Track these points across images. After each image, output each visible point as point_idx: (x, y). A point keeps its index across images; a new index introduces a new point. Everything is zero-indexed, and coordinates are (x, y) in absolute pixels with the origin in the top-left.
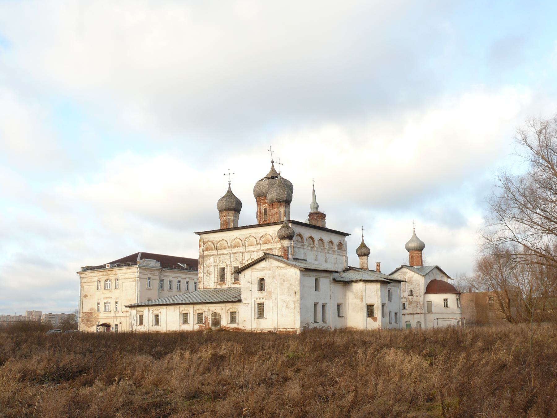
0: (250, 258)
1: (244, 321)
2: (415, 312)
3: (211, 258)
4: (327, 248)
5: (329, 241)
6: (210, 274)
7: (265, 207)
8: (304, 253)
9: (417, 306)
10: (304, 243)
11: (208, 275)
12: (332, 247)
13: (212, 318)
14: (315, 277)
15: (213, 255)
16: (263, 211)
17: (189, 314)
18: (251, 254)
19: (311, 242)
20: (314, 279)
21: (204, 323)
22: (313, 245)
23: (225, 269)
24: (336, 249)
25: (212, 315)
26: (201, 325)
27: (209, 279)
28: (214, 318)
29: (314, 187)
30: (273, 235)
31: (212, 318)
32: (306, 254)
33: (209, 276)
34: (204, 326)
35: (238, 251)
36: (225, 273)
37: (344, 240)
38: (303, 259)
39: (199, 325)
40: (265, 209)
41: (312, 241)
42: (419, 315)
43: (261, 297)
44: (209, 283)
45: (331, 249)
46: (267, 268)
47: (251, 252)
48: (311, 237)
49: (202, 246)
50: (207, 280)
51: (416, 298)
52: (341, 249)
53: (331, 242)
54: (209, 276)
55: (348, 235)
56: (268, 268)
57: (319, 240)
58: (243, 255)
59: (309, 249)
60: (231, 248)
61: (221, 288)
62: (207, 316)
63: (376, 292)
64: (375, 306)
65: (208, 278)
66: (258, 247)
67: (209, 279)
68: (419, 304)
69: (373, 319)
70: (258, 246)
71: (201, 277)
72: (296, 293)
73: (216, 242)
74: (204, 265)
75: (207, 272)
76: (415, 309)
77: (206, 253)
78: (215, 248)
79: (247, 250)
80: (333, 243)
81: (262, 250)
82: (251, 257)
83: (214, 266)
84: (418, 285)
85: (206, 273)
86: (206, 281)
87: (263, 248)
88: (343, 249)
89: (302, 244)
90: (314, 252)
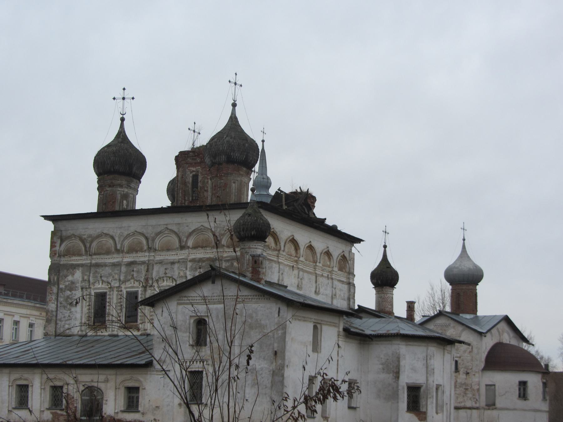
0: (164, 275)
1: (157, 407)
2: (462, 405)
3: (78, 271)
4: (321, 265)
5: (324, 251)
7: (194, 173)
8: (279, 272)
9: (466, 394)
10: (281, 252)
11: (68, 306)
12: (329, 263)
13: (83, 398)
14: (314, 322)
15: (82, 265)
16: (190, 179)
17: (30, 389)
18: (165, 267)
19: (293, 252)
20: (311, 326)
21: (64, 407)
22: (296, 257)
23: (108, 297)
24: (336, 269)
25: (84, 392)
26: (59, 412)
27: (69, 316)
28: (88, 398)
29: (263, 144)
30: (218, 230)
31: (83, 398)
32: (282, 274)
33: (70, 310)
34: (62, 415)
35: (137, 260)
36: (105, 304)
37: (350, 251)
38: (276, 282)
39: (52, 413)
40: (195, 177)
41: (293, 248)
42: (469, 411)
44: (69, 324)
45: (327, 268)
46: (215, 298)
47: (167, 264)
48: (294, 241)
49: (58, 245)
50: (64, 317)
51: (464, 376)
52: (344, 270)
53: (328, 254)
55: (359, 241)
56: (217, 298)
57: (307, 247)
58: (148, 269)
59: (288, 265)
60: (123, 252)
61: (96, 336)
62: (72, 394)
63: (425, 361)
64: (422, 390)
65: (67, 313)
66: (182, 255)
67: (69, 316)
68: (470, 390)
69: (417, 416)
70: (183, 252)
71: (52, 311)
72: (278, 355)
73: (90, 239)
74: (61, 286)
76: (460, 399)
77: (64, 261)
78: (86, 251)
79: (158, 258)
80: (331, 255)
81: (190, 261)
82: (166, 273)
83: (82, 289)
84: (470, 352)
86: (63, 319)
87: (194, 257)
88: (347, 270)
89: (275, 253)
90: (296, 272)
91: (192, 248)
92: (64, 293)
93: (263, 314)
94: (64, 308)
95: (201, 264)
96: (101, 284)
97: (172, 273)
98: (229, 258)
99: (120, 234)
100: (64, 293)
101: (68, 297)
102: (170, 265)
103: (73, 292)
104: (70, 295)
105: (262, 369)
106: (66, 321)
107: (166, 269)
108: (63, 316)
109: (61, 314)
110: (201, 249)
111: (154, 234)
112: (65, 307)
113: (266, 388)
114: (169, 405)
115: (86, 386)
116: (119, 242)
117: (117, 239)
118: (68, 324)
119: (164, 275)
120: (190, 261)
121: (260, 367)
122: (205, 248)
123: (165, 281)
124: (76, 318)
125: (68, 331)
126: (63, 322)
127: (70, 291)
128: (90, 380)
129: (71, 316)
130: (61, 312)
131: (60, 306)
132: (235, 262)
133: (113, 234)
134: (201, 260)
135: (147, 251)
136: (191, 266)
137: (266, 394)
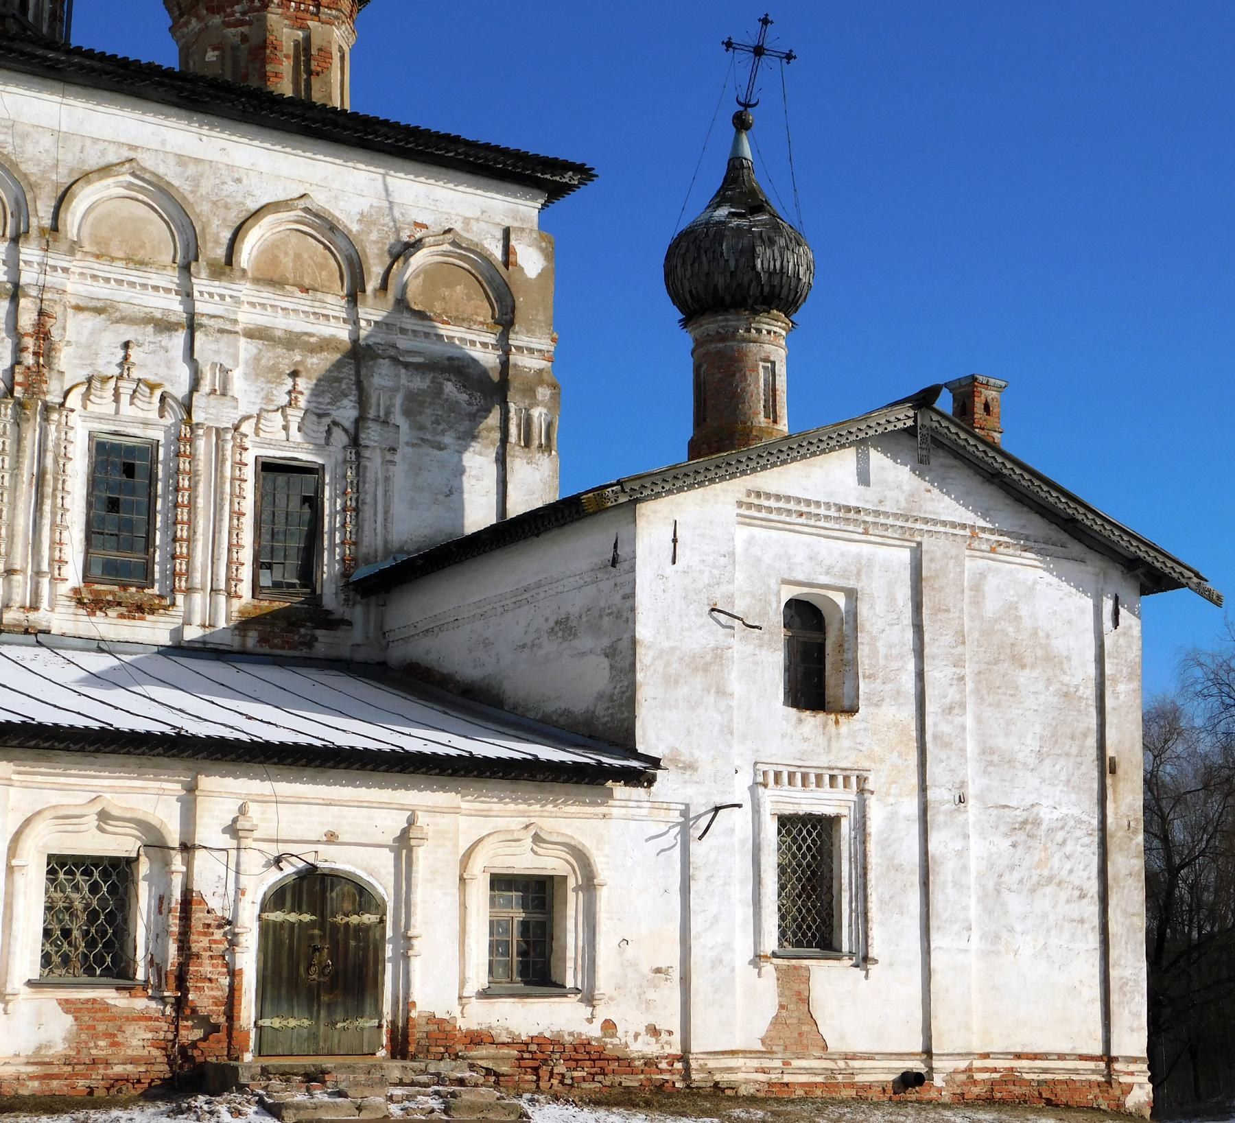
18: (129, 333)
26: (110, 996)
31: (276, 916)
43: (823, 761)
81: (251, 334)
91: (256, 281)
93: (1055, 613)
95: (298, 358)
97: (162, 371)
98: (421, 360)
102: (150, 328)
105: (1062, 823)
107: (126, 345)
111: (63, 170)
113: (1082, 897)
114: (721, 961)
120: (251, 334)
121: (1056, 815)
122: (319, 295)
128: (318, 834)
132: (449, 380)
134: (292, 341)
136: (257, 359)
137: (1082, 921)
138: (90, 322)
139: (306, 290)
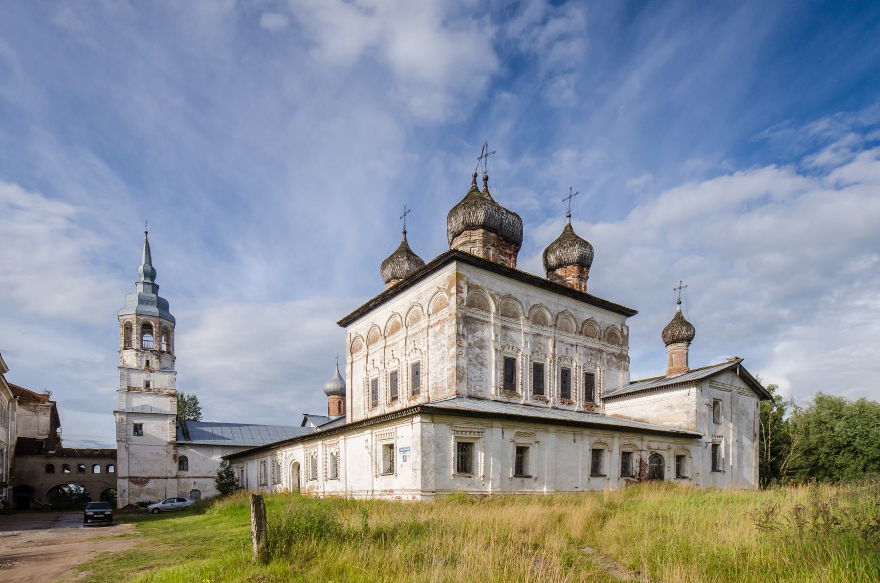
1: (698, 474)
6: (482, 364)
11: (479, 366)
18: (566, 346)
27: (480, 377)
28: (656, 465)
33: (481, 370)
44: (480, 386)
47: (567, 344)
50: (475, 377)
54: (481, 370)
62: (645, 461)
65: (478, 374)
66: (581, 340)
67: (480, 377)
75: (476, 359)
85: (474, 361)
92: (473, 349)
94: (475, 366)
96: (511, 349)
99: (526, 302)
100: (473, 349)
101: (478, 355)
102: (570, 346)
103: (483, 350)
104: (480, 353)
106: (477, 381)
108: (473, 376)
109: (471, 372)
110: (591, 338)
112: (475, 366)
115: (654, 453)
116: (526, 310)
117: (524, 305)
118: (479, 386)
119: (566, 355)
123: (566, 360)
124: (487, 380)
125: (479, 393)
126: (475, 382)
127: (480, 349)
129: (482, 376)
130: (471, 371)
131: (470, 364)
133: (521, 300)
135: (553, 327)
136: (585, 352)
138: (561, 344)
139: (592, 337)
